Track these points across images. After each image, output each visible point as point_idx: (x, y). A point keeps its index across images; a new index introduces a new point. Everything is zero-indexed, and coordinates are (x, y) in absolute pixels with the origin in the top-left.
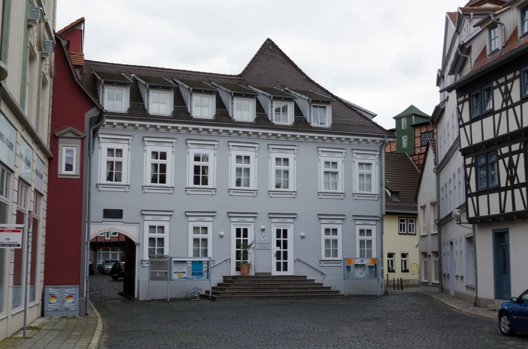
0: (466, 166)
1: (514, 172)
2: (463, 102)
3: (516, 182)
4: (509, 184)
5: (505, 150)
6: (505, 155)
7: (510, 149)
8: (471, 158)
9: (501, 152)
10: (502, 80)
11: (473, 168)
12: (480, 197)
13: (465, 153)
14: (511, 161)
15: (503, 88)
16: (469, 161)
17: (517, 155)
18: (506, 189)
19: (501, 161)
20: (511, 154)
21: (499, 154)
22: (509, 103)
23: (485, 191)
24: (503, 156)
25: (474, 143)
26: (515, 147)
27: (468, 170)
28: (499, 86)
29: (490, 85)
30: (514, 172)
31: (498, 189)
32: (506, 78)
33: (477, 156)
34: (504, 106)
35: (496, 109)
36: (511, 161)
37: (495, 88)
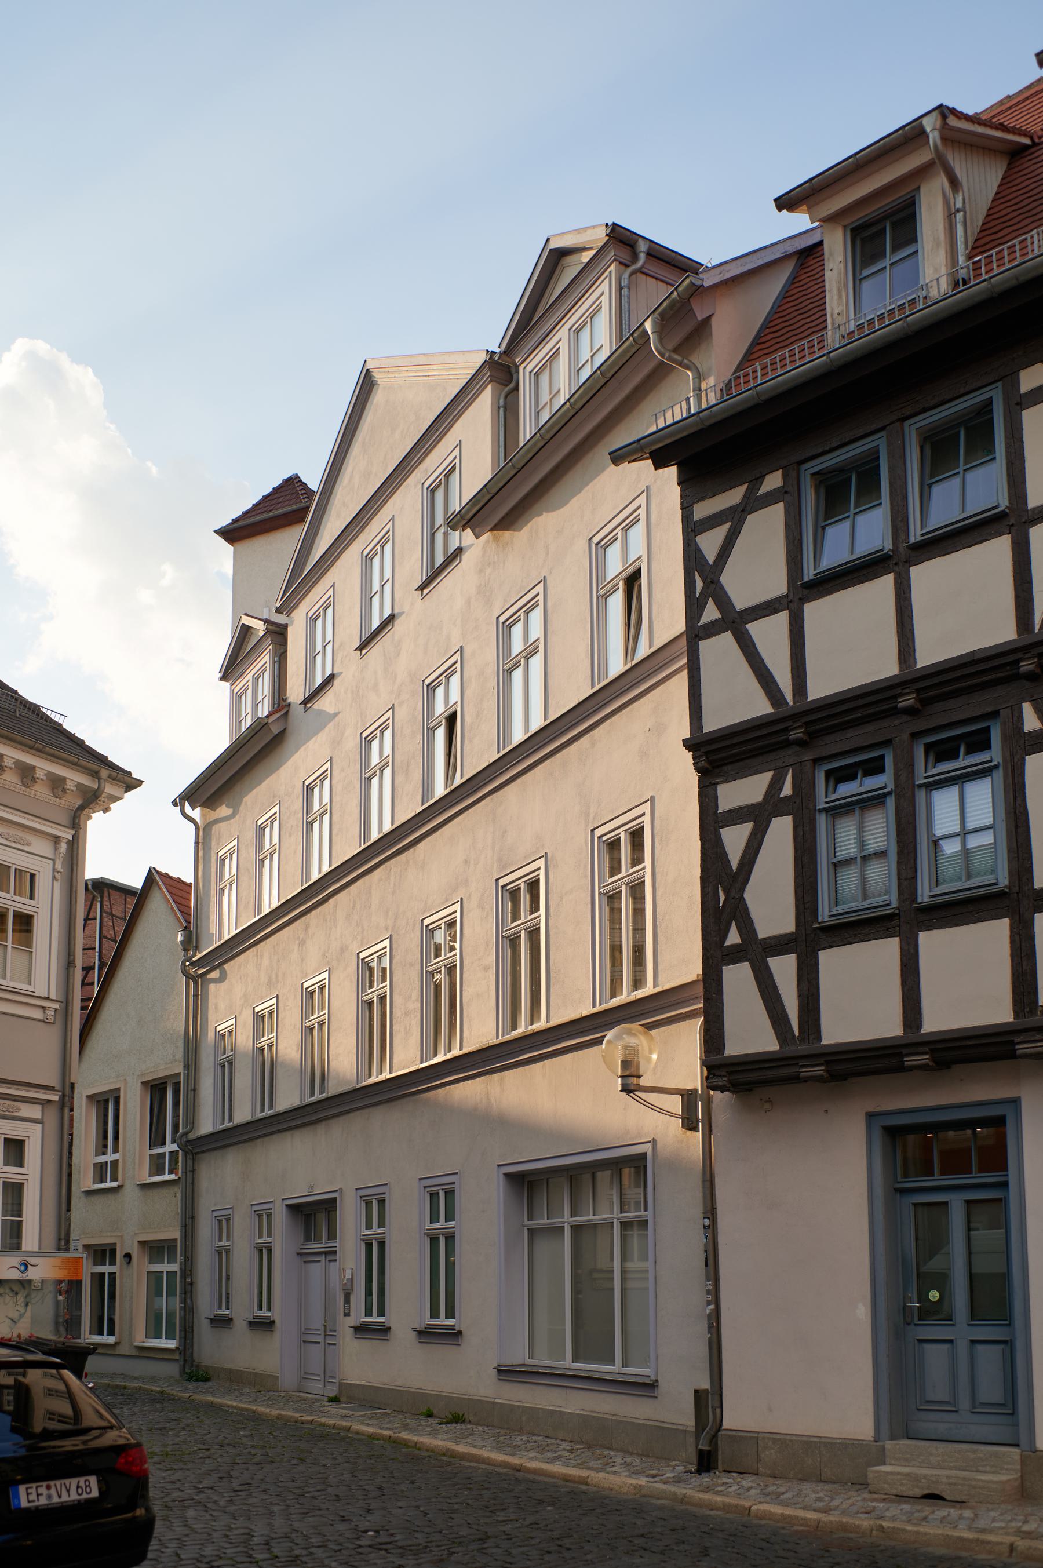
8: (766, 777)
12: (831, 961)
13: (717, 755)
16: (745, 790)
23: (890, 917)
25: (818, 689)
33: (817, 761)
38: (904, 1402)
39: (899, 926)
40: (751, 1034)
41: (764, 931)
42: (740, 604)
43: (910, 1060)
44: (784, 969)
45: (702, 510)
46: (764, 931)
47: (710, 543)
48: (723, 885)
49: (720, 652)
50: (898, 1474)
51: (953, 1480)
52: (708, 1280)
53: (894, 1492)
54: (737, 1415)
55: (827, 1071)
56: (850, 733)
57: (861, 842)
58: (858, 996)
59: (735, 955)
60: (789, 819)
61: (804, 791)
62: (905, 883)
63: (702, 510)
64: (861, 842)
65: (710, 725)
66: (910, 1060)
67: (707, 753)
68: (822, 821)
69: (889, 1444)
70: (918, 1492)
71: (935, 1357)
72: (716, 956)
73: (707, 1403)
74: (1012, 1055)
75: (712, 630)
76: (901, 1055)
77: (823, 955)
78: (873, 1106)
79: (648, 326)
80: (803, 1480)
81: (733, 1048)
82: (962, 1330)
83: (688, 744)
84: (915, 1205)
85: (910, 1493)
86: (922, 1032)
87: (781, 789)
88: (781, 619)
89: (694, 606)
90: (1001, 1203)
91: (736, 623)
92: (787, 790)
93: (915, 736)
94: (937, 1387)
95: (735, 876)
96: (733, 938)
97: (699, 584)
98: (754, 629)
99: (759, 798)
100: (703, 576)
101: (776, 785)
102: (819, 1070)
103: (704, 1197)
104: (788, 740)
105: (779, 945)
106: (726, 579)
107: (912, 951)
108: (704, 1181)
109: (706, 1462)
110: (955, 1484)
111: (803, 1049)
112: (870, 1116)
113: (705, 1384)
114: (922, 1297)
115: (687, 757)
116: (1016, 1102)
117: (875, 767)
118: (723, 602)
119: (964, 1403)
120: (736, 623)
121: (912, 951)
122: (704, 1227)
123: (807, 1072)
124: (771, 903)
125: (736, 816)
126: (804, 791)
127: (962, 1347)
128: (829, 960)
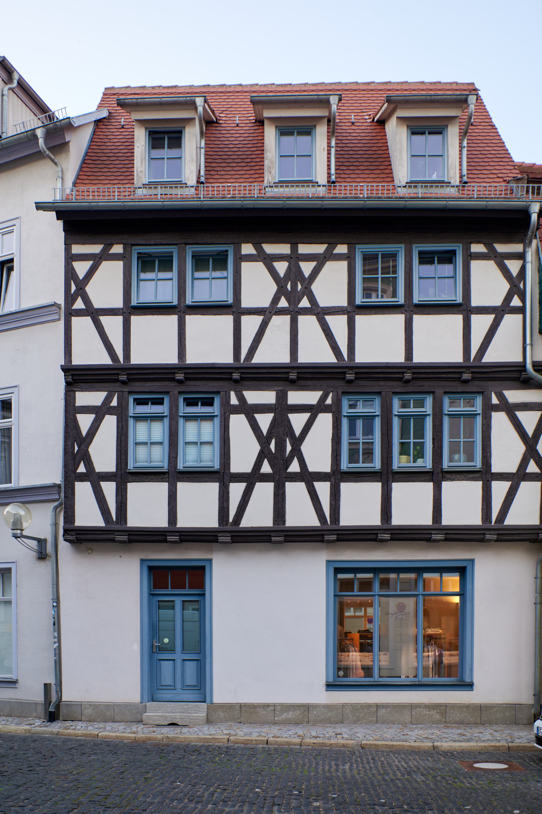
1: (289, 448)
3: (294, 467)
4: (266, 468)
5: (268, 397)
7: (282, 397)
9: (242, 399)
15: (281, 267)
18: (251, 479)
20: (281, 410)
21: (234, 401)
22: (305, 303)
26: (311, 397)
28: (269, 261)
30: (289, 448)
31: (222, 476)
34: (283, 303)
38: (154, 687)
39: (168, 478)
43: (169, 538)
49: (82, 326)
50: (158, 716)
51: (183, 717)
52: (54, 631)
53: (156, 723)
54: (70, 694)
55: (128, 539)
56: (149, 384)
60: (114, 418)
62: (172, 459)
66: (169, 538)
67: (72, 375)
68: (131, 421)
69: (148, 704)
70: (167, 723)
76: (166, 535)
78: (143, 556)
80: (105, 722)
84: (159, 601)
85: (163, 724)
86: (177, 526)
87: (111, 402)
91: (94, 314)
92: (114, 403)
99: (99, 404)
101: (108, 399)
102: (125, 538)
103: (53, 592)
104: (118, 379)
107: (174, 490)
108: (53, 584)
109: (52, 717)
110: (183, 719)
113: (51, 680)
117: (160, 402)
120: (94, 314)
121: (174, 490)
122: (54, 606)
123: (118, 538)
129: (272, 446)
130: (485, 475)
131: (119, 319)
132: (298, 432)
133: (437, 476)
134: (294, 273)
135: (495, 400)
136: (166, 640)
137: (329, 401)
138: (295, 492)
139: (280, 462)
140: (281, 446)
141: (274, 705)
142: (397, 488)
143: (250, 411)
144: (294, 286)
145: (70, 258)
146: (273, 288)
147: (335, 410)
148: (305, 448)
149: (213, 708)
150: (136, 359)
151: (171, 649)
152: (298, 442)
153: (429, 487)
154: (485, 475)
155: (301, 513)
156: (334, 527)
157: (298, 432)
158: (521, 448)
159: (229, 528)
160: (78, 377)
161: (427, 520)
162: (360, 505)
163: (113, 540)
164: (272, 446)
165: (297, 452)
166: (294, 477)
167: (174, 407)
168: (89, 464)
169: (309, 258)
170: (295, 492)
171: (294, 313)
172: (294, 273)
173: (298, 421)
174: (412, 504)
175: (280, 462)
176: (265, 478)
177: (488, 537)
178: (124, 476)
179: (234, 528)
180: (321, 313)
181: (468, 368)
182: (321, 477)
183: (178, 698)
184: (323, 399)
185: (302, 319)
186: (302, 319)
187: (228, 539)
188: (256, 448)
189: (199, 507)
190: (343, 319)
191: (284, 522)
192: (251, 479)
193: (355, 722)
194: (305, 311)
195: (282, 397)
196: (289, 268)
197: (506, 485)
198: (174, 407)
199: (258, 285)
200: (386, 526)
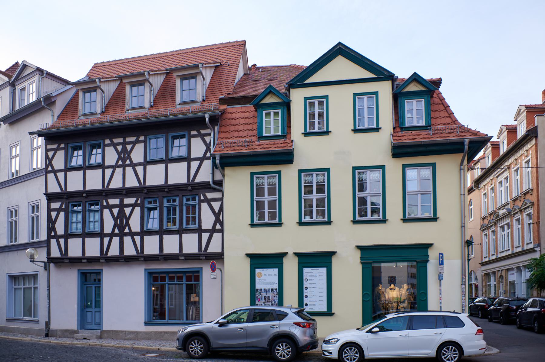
0: (49, 210)
1: (125, 222)
2: (56, 150)
3: (127, 230)
4: (117, 231)
5: (116, 201)
6: (115, 206)
7: (122, 201)
8: (59, 204)
9: (107, 203)
10: (121, 140)
11: (62, 214)
13: (51, 197)
14: (121, 213)
15: (120, 148)
16: (55, 205)
17: (130, 208)
18: (111, 235)
19: (106, 212)
20: (122, 206)
21: (105, 204)
22: (128, 162)
24: (110, 207)
26: (132, 201)
27: (54, 214)
28: (115, 145)
29: (102, 142)
30: (125, 222)
31: (101, 235)
32: (124, 140)
33: (69, 202)
34: (120, 163)
35: (107, 164)
36: (121, 213)
37: (108, 145)
38: (83, 323)
40: (55, 253)
41: (58, 234)
42: (56, 168)
43: (83, 261)
44: (62, 241)
45: (49, 147)
46: (58, 234)
47: (50, 154)
48: (51, 223)
49: (51, 176)
57: (77, 220)
58: (75, 248)
59: (53, 237)
61: (67, 207)
63: (49, 147)
64: (77, 220)
65: (49, 191)
66: (83, 261)
68: (70, 214)
71: (89, 314)
72: (49, 237)
73: (48, 324)
74: (100, 262)
75: (50, 172)
77: (69, 240)
79: (42, 99)
81: (52, 255)
82: (93, 310)
83: (45, 194)
88: (63, 173)
89: (47, 166)
90: (100, 287)
91: (55, 172)
92: (64, 207)
93: (86, 201)
94: (89, 320)
95: (53, 222)
96: (53, 234)
97: (48, 162)
98: (58, 174)
99: (58, 207)
100: (49, 161)
101: (61, 205)
105: (61, 237)
106: (53, 162)
109: (47, 335)
111: (65, 257)
112: (78, 270)
113: (47, 321)
114: (87, 304)
115: (45, 196)
116: (102, 269)
118: (52, 167)
119: (94, 323)
120: (55, 172)
123: (66, 261)
124: (60, 228)
125: (54, 210)
126: (67, 207)
127: (94, 313)
128: (70, 240)
129: (119, 222)
130: (199, 231)
131: (63, 173)
132: (128, 215)
133: (180, 232)
134: (124, 149)
135: (202, 198)
136: (89, 303)
137: (139, 202)
138: (127, 240)
139: (121, 228)
140: (121, 222)
141: (125, 331)
142: (166, 237)
143: (110, 207)
144: (124, 155)
145: (47, 150)
146: (117, 156)
147: (142, 206)
148: (130, 222)
149: (103, 332)
150: (69, 189)
151: (90, 307)
152: (128, 219)
153: (177, 236)
154: (199, 231)
155: (130, 250)
156: (142, 255)
157: (128, 216)
158: (213, 218)
159: (104, 256)
160: (51, 197)
161: (177, 251)
162: (151, 245)
163: (63, 262)
164: (119, 222)
165: (128, 224)
166: (127, 234)
167: (84, 207)
168: (55, 232)
169: (129, 143)
170: (127, 240)
171: (124, 166)
172: (124, 149)
173: (128, 210)
174: (171, 244)
175: (121, 228)
176: (116, 235)
177: (201, 258)
178: (67, 236)
179: (106, 256)
180: (133, 165)
181: (189, 185)
182: (137, 234)
183: (93, 328)
184: (137, 201)
185: (127, 168)
186: (127, 168)
187: (104, 261)
188: (113, 222)
189: (93, 248)
190: (142, 168)
191: (123, 253)
192: (111, 235)
193: (155, 340)
194: (128, 165)
195: (122, 201)
196: (122, 148)
197: (208, 235)
198: (84, 207)
199: (111, 156)
200: (161, 254)
